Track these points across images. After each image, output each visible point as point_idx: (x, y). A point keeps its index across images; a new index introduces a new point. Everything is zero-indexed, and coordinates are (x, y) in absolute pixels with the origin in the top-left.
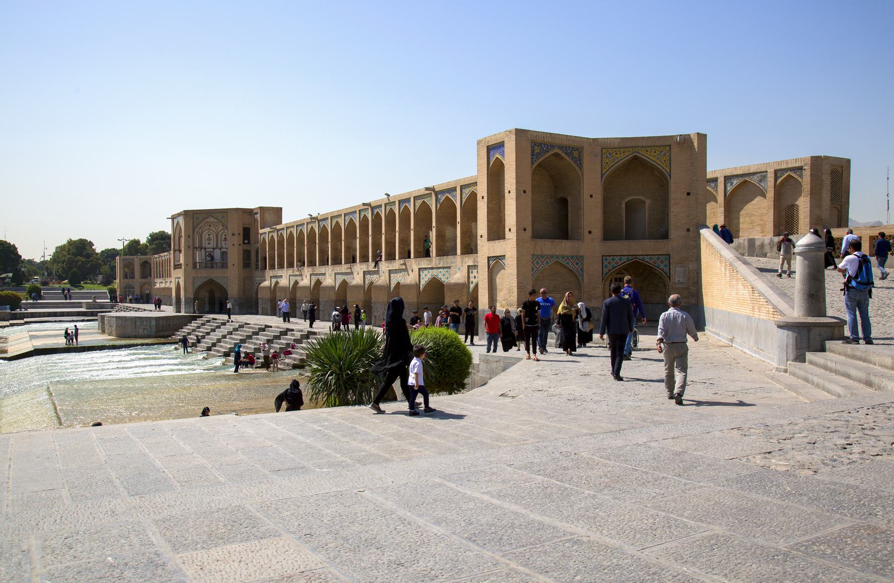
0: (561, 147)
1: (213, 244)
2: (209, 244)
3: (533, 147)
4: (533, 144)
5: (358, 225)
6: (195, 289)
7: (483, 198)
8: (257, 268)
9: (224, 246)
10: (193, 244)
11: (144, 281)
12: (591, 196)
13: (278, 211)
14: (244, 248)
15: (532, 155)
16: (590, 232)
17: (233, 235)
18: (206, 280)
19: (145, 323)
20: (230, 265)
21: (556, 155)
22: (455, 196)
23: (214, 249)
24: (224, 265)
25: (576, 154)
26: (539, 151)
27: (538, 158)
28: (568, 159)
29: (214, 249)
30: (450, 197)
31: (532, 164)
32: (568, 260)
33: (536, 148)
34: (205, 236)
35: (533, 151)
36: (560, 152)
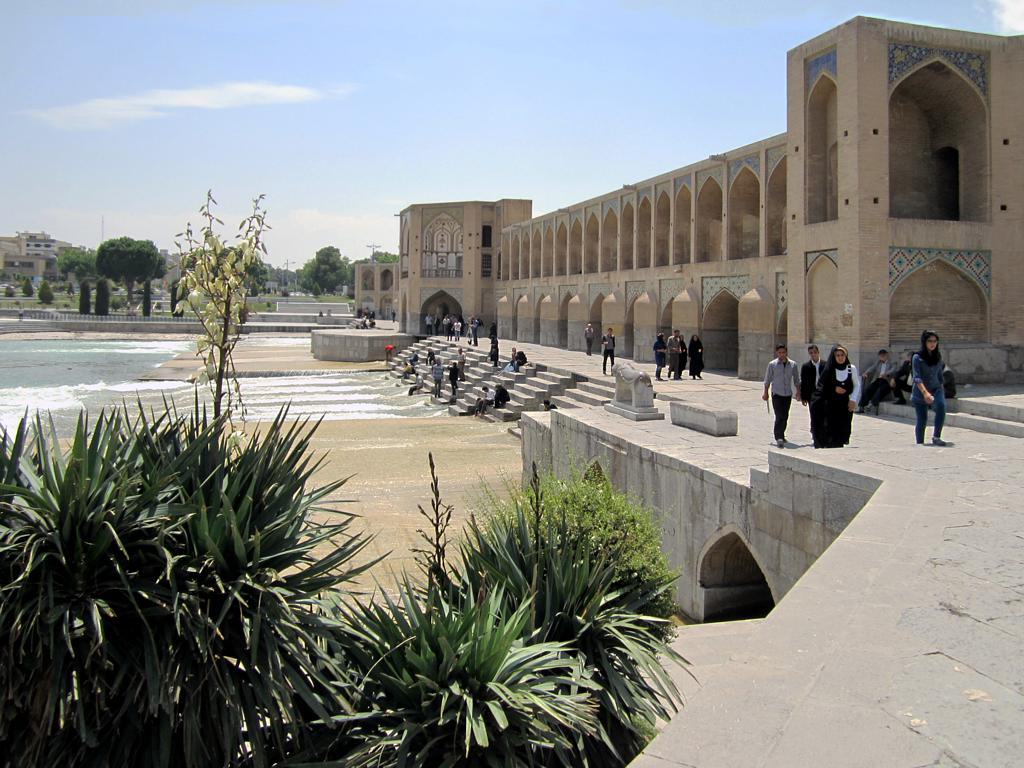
0: (946, 53)
1: (447, 247)
2: (442, 246)
3: (891, 52)
4: (892, 47)
5: (619, 216)
6: (423, 302)
7: (797, 149)
8: (499, 278)
9: (460, 249)
10: (422, 246)
11: (384, 292)
12: (1006, 142)
13: (526, 205)
14: (485, 252)
15: (890, 66)
16: (1004, 208)
17: (470, 235)
18: (435, 292)
19: (356, 344)
20: (465, 274)
21: (937, 68)
22: (757, 166)
23: (448, 253)
24: (459, 272)
25: (975, 65)
26: (903, 59)
27: (901, 71)
28: (960, 74)
29: (448, 253)
30: (750, 168)
31: (891, 81)
32: (960, 258)
33: (898, 53)
34: (437, 237)
35: (892, 59)
36: (944, 62)
